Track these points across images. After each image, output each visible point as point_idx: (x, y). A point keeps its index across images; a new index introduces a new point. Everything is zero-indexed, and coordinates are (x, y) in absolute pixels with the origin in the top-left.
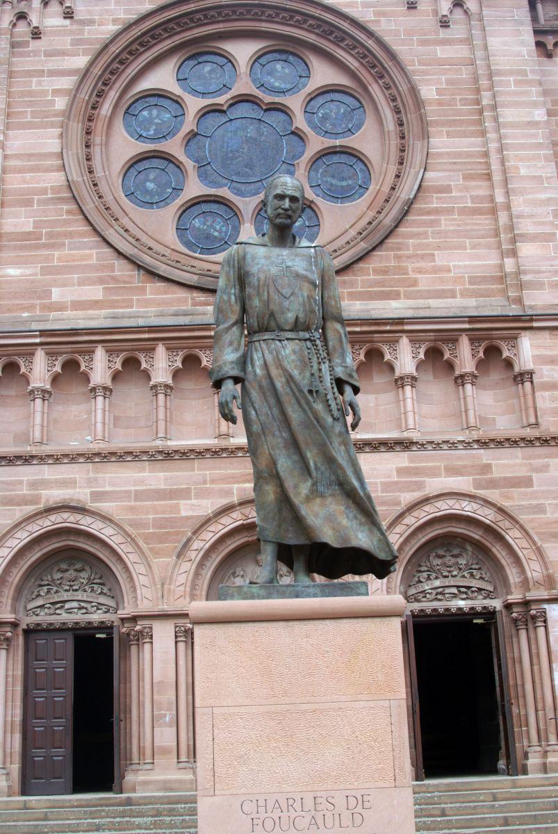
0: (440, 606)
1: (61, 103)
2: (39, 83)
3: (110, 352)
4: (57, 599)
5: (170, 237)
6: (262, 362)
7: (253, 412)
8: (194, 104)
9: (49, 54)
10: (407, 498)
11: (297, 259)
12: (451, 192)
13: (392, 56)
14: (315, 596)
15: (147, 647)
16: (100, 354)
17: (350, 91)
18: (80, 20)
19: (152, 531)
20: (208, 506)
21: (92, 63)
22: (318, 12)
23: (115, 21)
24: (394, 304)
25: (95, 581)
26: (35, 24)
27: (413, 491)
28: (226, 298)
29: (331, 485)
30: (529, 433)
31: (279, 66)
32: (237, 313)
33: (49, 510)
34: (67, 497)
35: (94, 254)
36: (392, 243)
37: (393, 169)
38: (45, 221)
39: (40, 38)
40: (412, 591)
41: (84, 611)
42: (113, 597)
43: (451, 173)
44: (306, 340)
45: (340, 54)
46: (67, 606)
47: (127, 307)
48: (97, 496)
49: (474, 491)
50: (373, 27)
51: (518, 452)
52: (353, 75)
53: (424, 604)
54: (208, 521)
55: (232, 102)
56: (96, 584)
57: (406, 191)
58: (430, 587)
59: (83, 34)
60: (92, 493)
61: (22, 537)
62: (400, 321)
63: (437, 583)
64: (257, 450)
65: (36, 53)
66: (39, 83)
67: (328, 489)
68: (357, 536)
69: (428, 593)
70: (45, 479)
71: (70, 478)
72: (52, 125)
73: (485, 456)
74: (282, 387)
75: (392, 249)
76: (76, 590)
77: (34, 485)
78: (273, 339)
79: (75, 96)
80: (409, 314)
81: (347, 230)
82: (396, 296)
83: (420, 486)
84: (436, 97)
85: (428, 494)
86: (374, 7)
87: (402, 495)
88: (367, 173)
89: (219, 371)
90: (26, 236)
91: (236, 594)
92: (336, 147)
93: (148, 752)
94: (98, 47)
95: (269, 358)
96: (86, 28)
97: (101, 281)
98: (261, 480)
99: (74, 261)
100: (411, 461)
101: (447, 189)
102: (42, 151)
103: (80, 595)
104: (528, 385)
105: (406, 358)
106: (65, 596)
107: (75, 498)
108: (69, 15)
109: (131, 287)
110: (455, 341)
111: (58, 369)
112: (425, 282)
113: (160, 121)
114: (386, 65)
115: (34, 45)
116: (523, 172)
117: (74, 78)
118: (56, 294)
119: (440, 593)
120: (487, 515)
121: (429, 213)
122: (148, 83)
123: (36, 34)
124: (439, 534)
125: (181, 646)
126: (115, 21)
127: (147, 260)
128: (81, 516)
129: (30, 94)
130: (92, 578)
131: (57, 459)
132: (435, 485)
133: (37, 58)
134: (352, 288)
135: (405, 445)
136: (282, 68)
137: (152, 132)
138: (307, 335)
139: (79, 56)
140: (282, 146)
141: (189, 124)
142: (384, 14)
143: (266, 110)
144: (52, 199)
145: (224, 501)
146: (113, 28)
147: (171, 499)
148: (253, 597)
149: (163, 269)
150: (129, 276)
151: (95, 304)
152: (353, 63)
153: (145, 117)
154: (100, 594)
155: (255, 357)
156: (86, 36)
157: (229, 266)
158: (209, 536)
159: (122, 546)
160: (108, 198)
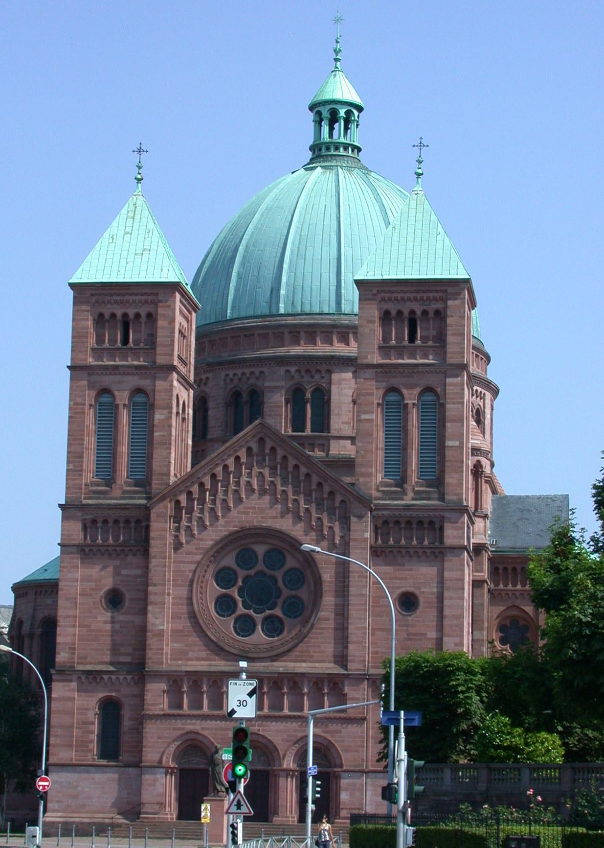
21: (202, 559)
23: (211, 540)
24: (304, 665)
33: (188, 733)
48: (203, 729)
66: (183, 567)
90: (181, 631)
106: (193, 759)
118: (190, 655)
126: (211, 540)
127: (221, 644)
146: (211, 543)
149: (226, 648)
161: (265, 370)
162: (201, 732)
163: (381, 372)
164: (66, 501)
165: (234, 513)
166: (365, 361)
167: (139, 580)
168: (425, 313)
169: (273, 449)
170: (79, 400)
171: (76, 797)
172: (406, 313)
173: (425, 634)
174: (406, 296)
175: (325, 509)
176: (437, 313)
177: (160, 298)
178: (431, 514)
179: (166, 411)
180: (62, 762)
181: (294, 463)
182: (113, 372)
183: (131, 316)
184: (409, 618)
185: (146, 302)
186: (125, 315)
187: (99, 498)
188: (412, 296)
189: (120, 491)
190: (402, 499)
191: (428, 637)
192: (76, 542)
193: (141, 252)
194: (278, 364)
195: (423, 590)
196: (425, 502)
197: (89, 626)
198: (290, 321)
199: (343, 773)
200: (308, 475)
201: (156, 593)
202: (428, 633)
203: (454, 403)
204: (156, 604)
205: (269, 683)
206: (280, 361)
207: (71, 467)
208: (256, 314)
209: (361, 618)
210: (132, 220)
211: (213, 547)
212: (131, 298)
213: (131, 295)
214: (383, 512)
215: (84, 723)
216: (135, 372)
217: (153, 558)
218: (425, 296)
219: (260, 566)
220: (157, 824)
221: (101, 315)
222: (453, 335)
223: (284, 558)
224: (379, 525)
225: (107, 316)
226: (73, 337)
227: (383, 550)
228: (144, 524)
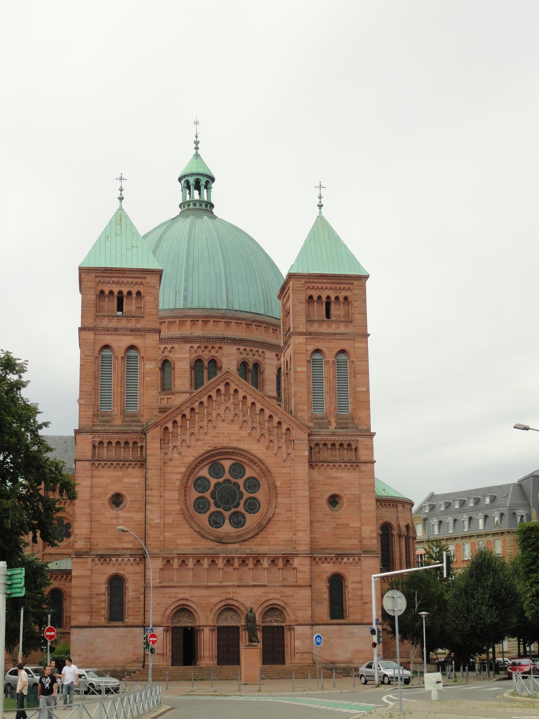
0: (270, 624)
1: (178, 483)
3: (193, 559)
5: (207, 523)
8: (213, 481)
9: (175, 466)
10: (264, 599)
13: (269, 471)
15: (202, 633)
16: (191, 560)
20: (217, 600)
23: (192, 456)
24: (264, 547)
26: (170, 457)
30: (295, 584)
33: (180, 600)
35: (188, 530)
40: (264, 621)
45: (254, 467)
48: (191, 597)
49: (280, 598)
51: (291, 589)
54: (217, 603)
57: (269, 515)
61: (174, 606)
62: (265, 554)
63: (270, 619)
72: (176, 490)
73: (283, 589)
77: (176, 593)
82: (265, 545)
93: (203, 657)
97: (190, 538)
101: (280, 514)
103: (185, 619)
104: (295, 571)
105: (266, 563)
106: (182, 619)
108: (180, 453)
110: (278, 559)
111: (180, 563)
115: (170, 463)
116: (301, 511)
118: (179, 542)
119: (271, 621)
120: (282, 604)
121: (275, 521)
125: (210, 633)
126: (192, 456)
127: (202, 532)
131: (181, 587)
132: (271, 596)
135: (264, 586)
145: (221, 599)
151: (189, 545)
158: (218, 607)
161: (176, 346)
163: (309, 338)
164: (79, 428)
165: (208, 437)
166: (298, 330)
167: (137, 486)
168: (337, 298)
169: (236, 391)
170: (88, 353)
171: (93, 651)
172: (324, 298)
173: (348, 524)
174: (324, 286)
175: (275, 435)
176: (346, 298)
177: (147, 280)
178: (350, 439)
179: (154, 363)
180: (82, 624)
181: (253, 400)
182: (113, 333)
183: (125, 293)
184: (337, 513)
185: (137, 283)
186: (120, 292)
187: (105, 426)
188: (329, 286)
189: (121, 421)
190: (328, 428)
191: (351, 526)
192: (89, 458)
193: (131, 248)
194: (185, 342)
195: (345, 492)
196: (344, 430)
197: (100, 521)
198: (191, 313)
199: (296, 626)
200: (262, 410)
201: (152, 496)
202: (351, 524)
203: (361, 361)
204: (152, 504)
205: (239, 562)
206: (186, 340)
207: (83, 402)
208: (165, 308)
209: (305, 513)
210: (120, 226)
211: (193, 461)
212: (125, 280)
213: (126, 277)
214: (316, 437)
215: (98, 594)
216: (130, 333)
217: (149, 470)
218: (337, 286)
219: (227, 476)
220: (162, 670)
221: (102, 292)
222: (359, 314)
223: (245, 470)
224: (313, 446)
225: (107, 293)
226: (82, 307)
227: (317, 464)
228: (139, 445)
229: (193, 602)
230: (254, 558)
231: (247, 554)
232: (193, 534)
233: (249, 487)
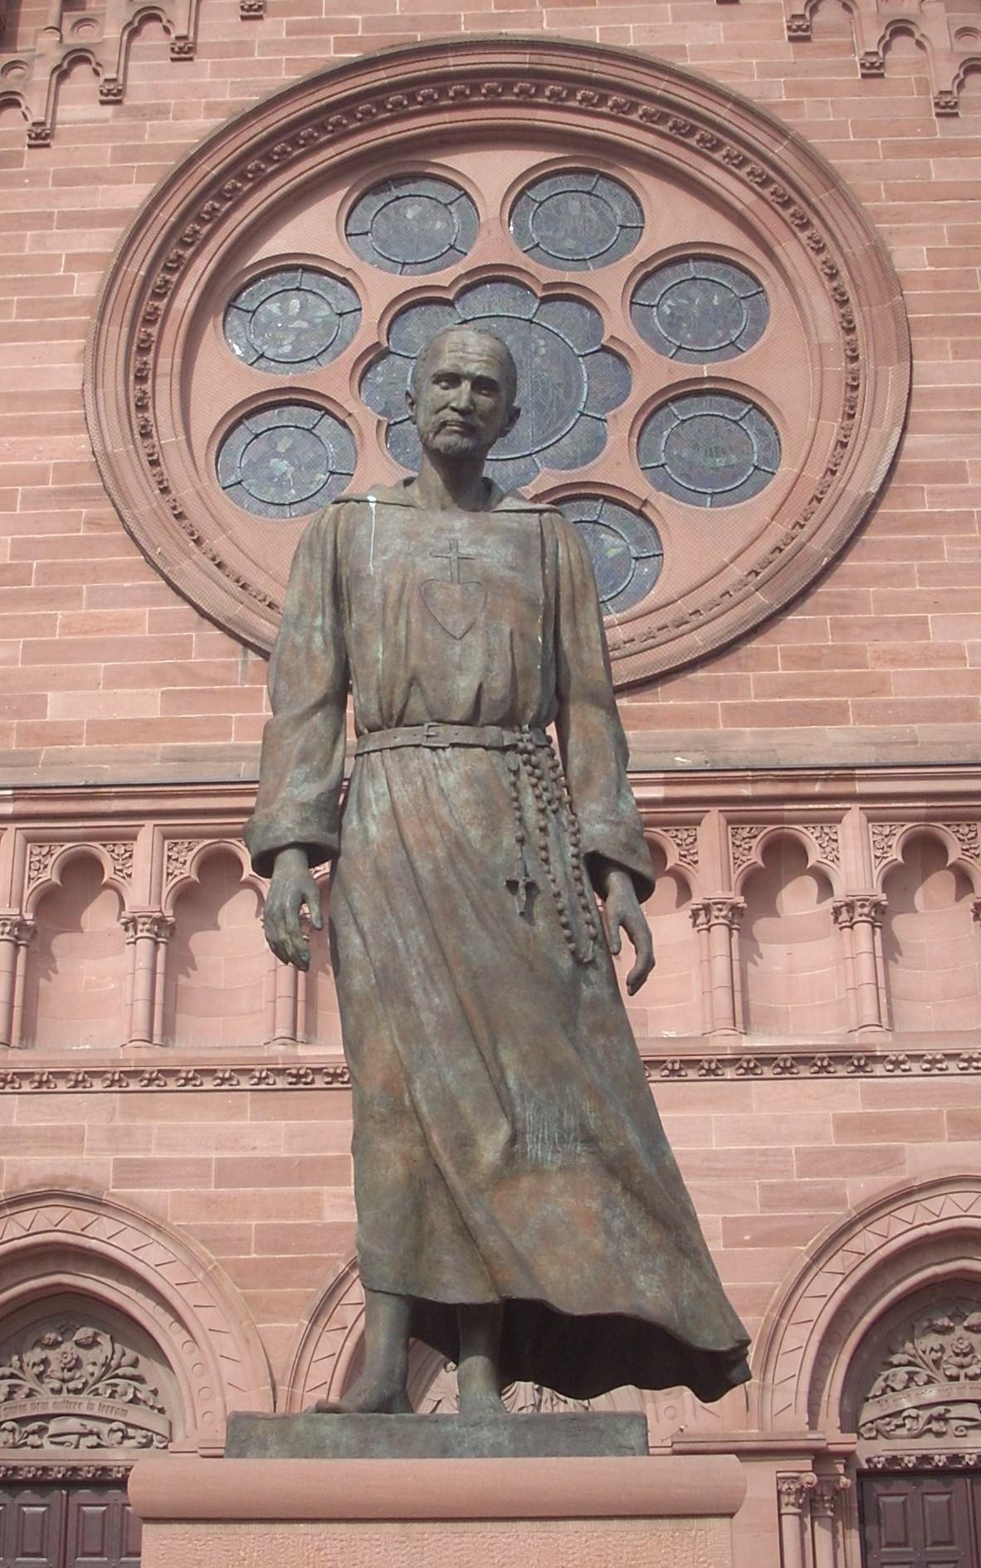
0: (938, 1449)
1: (86, 285)
2: (39, 242)
4: (29, 1412)
6: (385, 805)
7: (357, 941)
9: (62, 180)
10: (860, 1188)
11: (490, 539)
12: (965, 480)
13: (830, 179)
14: (497, 1452)
17: (726, 255)
18: (135, 107)
19: (254, 1256)
21: (157, 200)
22: (663, 85)
23: (211, 109)
25: (120, 1372)
27: (875, 1172)
28: (300, 640)
29: (562, 1140)
31: (574, 205)
32: (326, 678)
34: (61, 1171)
36: (828, 594)
37: (831, 429)
38: (39, 542)
39: (48, 146)
41: (93, 1440)
42: (161, 1411)
43: (965, 437)
44: (504, 750)
46: (54, 1427)
47: (215, 737)
48: (130, 1172)
50: (786, 119)
52: (740, 221)
53: (899, 1444)
55: (465, 282)
56: (124, 1377)
57: (863, 479)
58: (915, 1403)
59: (141, 138)
60: (120, 1165)
62: (846, 772)
64: (361, 1042)
65: (37, 177)
66: (39, 242)
67: (555, 1152)
68: (630, 1284)
69: (909, 1416)
70: (11, 1129)
71: (70, 1128)
72: (64, 332)
74: (436, 871)
75: (829, 608)
76: (77, 1391)
78: (417, 746)
79: (117, 268)
80: (868, 756)
81: (727, 566)
82: (838, 715)
83: (891, 1160)
84: (928, 268)
85: (908, 1180)
86: (786, 75)
87: (849, 1180)
88: (773, 437)
89: (267, 828)
91: (272, 1438)
92: (701, 380)
94: (173, 164)
95: (403, 795)
96: (148, 123)
97: (159, 676)
98: (370, 1124)
99: (98, 631)
100: (870, 1097)
102: (38, 389)
103: (84, 1403)
107: (80, 1175)
108: (113, 96)
109: (224, 693)
112: (904, 686)
113: (305, 325)
114: (814, 200)
117: (115, 229)
118: (57, 706)
121: (914, 524)
122: (276, 245)
123: (41, 137)
124: (936, 1276)
126: (211, 109)
128: (91, 1217)
129: (20, 264)
130: (114, 1363)
133: (37, 189)
134: (734, 697)
136: (583, 207)
137: (287, 349)
138: (508, 738)
139: (130, 182)
140: (579, 379)
141: (367, 333)
142: (810, 90)
143: (544, 300)
144: (55, 492)
147: (302, 1182)
148: (317, 1450)
150: (223, 665)
151: (146, 729)
152: (740, 195)
153: (270, 313)
154: (131, 1401)
155: (370, 793)
156: (147, 140)
157: (312, 557)
159: (185, 1291)
160: (184, 491)
162: (115, 1192)
229: (151, 1223)
230: (739, 813)
231: (674, 777)
232: (183, 648)
233: (672, 323)
